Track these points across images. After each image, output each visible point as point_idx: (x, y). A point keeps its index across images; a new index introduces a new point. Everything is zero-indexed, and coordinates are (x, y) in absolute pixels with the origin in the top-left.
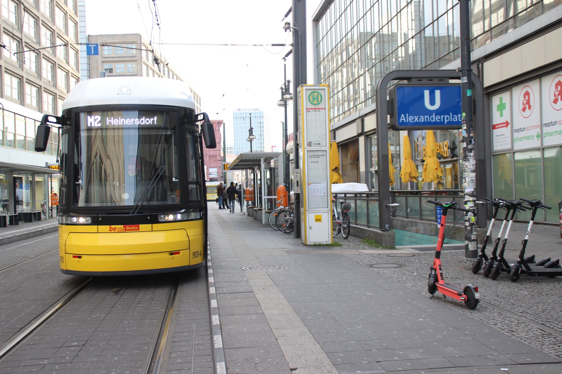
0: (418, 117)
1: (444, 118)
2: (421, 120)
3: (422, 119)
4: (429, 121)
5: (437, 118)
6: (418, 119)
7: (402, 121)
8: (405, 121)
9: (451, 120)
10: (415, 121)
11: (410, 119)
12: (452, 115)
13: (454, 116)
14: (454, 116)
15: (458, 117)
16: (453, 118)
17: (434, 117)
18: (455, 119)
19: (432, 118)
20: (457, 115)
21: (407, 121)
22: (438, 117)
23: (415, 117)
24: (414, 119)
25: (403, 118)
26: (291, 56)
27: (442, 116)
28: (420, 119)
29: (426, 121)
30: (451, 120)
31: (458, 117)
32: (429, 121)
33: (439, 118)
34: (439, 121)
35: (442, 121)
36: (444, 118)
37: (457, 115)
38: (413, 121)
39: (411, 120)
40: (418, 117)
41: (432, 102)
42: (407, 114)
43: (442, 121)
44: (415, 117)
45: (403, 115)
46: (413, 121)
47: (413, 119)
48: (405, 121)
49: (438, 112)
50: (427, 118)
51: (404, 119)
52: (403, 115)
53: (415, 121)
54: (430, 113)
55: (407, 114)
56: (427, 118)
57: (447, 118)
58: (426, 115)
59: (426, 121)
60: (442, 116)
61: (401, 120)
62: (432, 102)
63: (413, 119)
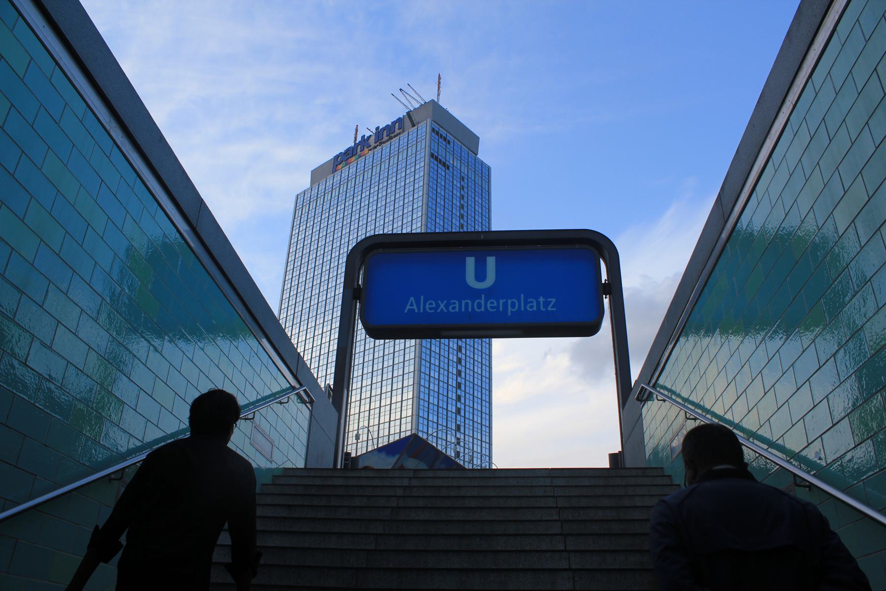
0: (445, 302)
1: (505, 305)
2: (454, 308)
3: (456, 307)
4: (470, 310)
5: (489, 305)
6: (447, 306)
7: (409, 309)
9: (523, 309)
10: (439, 311)
11: (427, 306)
13: (529, 300)
14: (529, 300)
15: (538, 303)
16: (526, 303)
17: (483, 302)
18: (532, 307)
19: (479, 306)
20: (537, 299)
21: (422, 311)
22: (492, 303)
23: (439, 302)
24: (438, 306)
25: (412, 305)
26: (165, 434)
27: (501, 302)
28: (451, 307)
29: (463, 310)
30: (523, 309)
31: (538, 303)
32: (470, 310)
33: (495, 305)
34: (495, 310)
35: (501, 309)
36: (505, 304)
37: (537, 299)
38: (433, 311)
39: (430, 309)
40: (445, 302)
41: (481, 275)
42: (422, 297)
43: (501, 309)
44: (439, 302)
45: (412, 299)
46: (433, 311)
47: (434, 305)
49: (489, 293)
50: (467, 304)
51: (415, 307)
52: (412, 299)
53: (439, 311)
54: (475, 294)
55: (422, 297)
56: (467, 304)
57: (513, 305)
58: (465, 300)
59: (463, 310)
61: (408, 307)
62: (481, 275)
63: (434, 305)
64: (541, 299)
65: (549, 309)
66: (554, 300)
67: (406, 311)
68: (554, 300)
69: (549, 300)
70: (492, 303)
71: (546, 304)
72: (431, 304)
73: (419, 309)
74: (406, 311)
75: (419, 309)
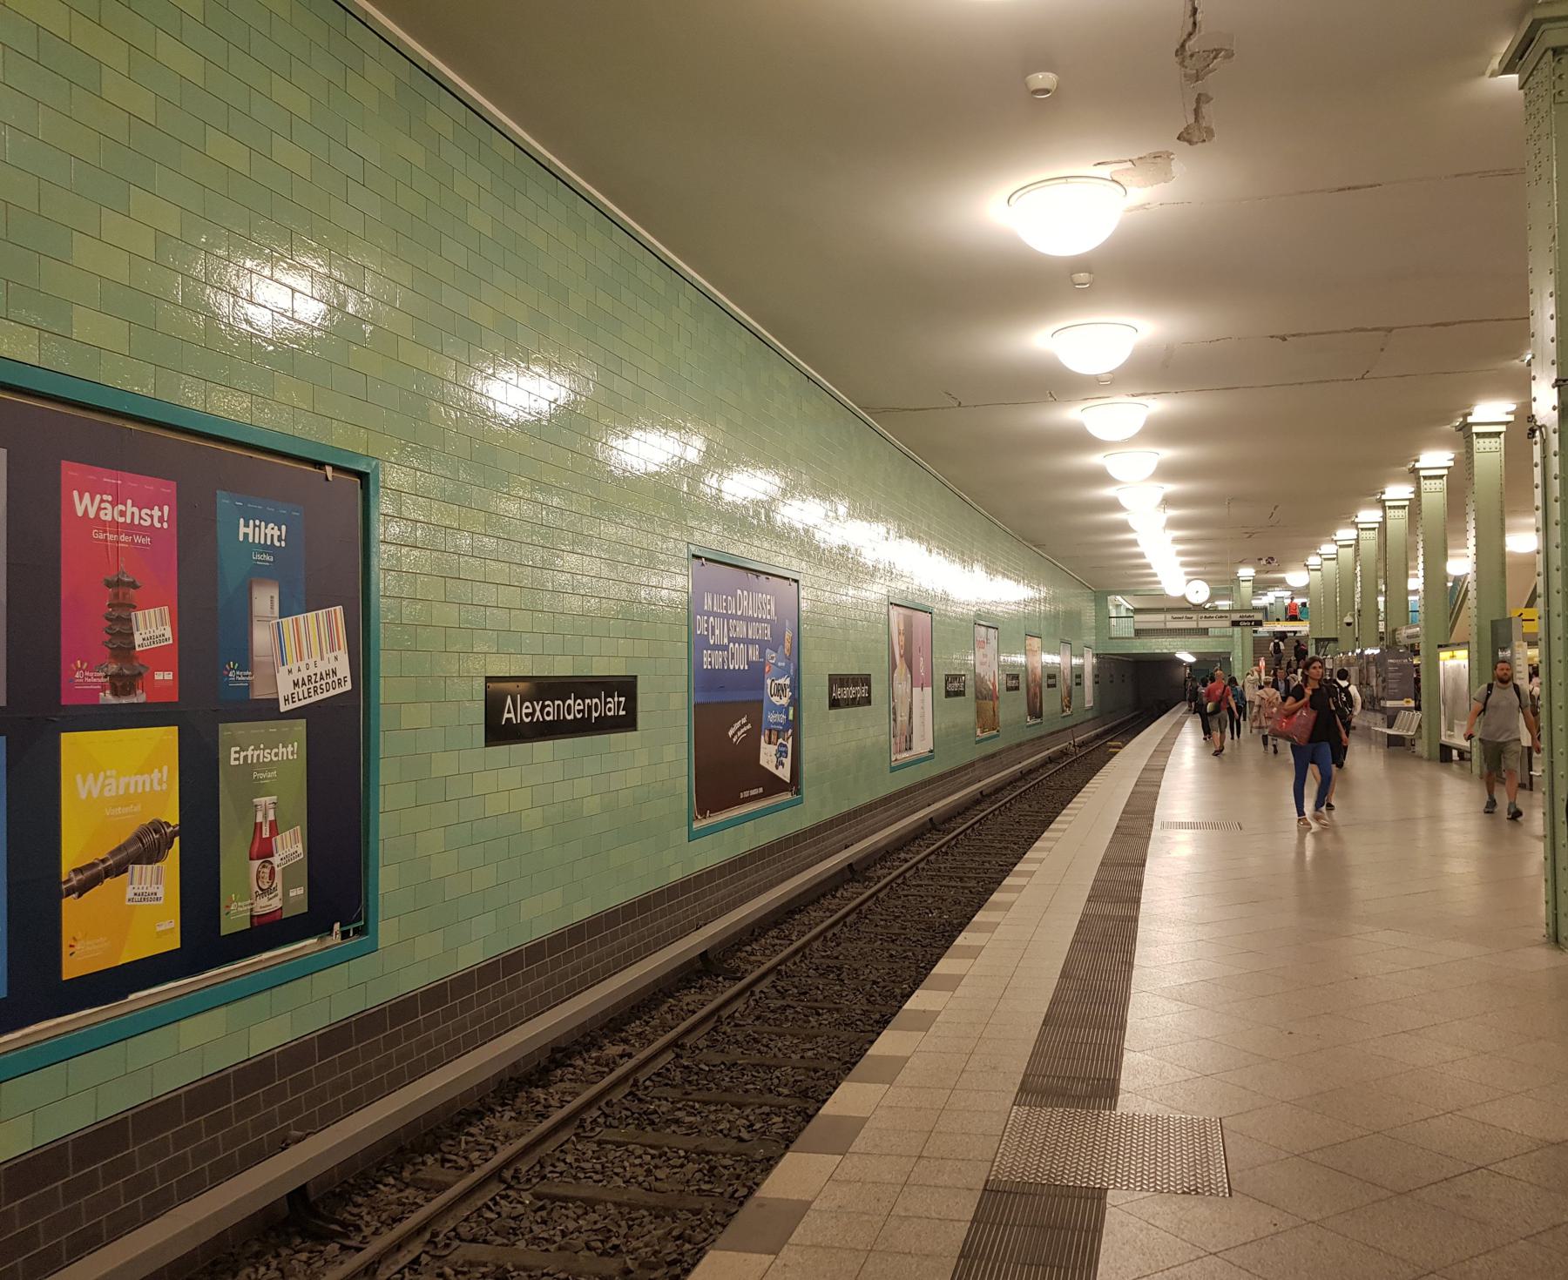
1: (590, 707)
4: (562, 718)
6: (542, 711)
7: (507, 719)
8: (515, 722)
12: (605, 700)
21: (519, 721)
22: (579, 705)
25: (509, 712)
33: (581, 707)
39: (527, 715)
48: (515, 722)
50: (559, 705)
51: (512, 715)
60: (588, 701)
61: (506, 715)
63: (530, 710)
64: (616, 699)
65: (622, 713)
66: (623, 699)
67: (503, 723)
68: (623, 699)
69: (621, 699)
70: (579, 705)
71: (619, 703)
72: (527, 707)
73: (516, 720)
74: (503, 723)
75: (516, 720)
